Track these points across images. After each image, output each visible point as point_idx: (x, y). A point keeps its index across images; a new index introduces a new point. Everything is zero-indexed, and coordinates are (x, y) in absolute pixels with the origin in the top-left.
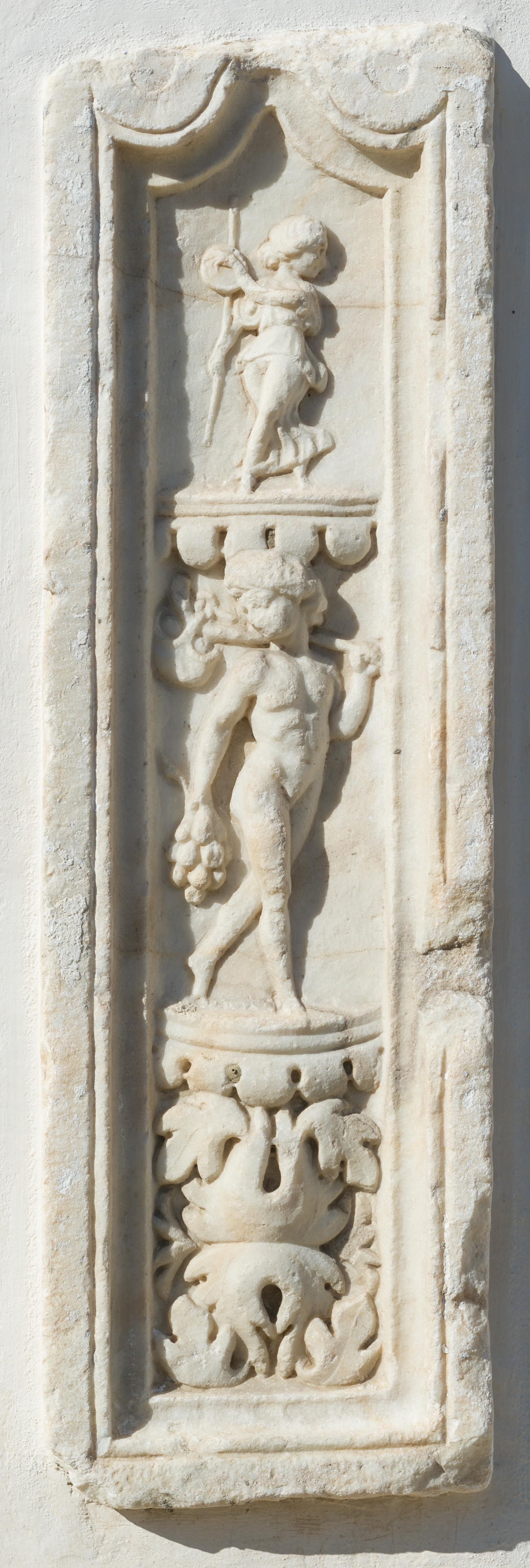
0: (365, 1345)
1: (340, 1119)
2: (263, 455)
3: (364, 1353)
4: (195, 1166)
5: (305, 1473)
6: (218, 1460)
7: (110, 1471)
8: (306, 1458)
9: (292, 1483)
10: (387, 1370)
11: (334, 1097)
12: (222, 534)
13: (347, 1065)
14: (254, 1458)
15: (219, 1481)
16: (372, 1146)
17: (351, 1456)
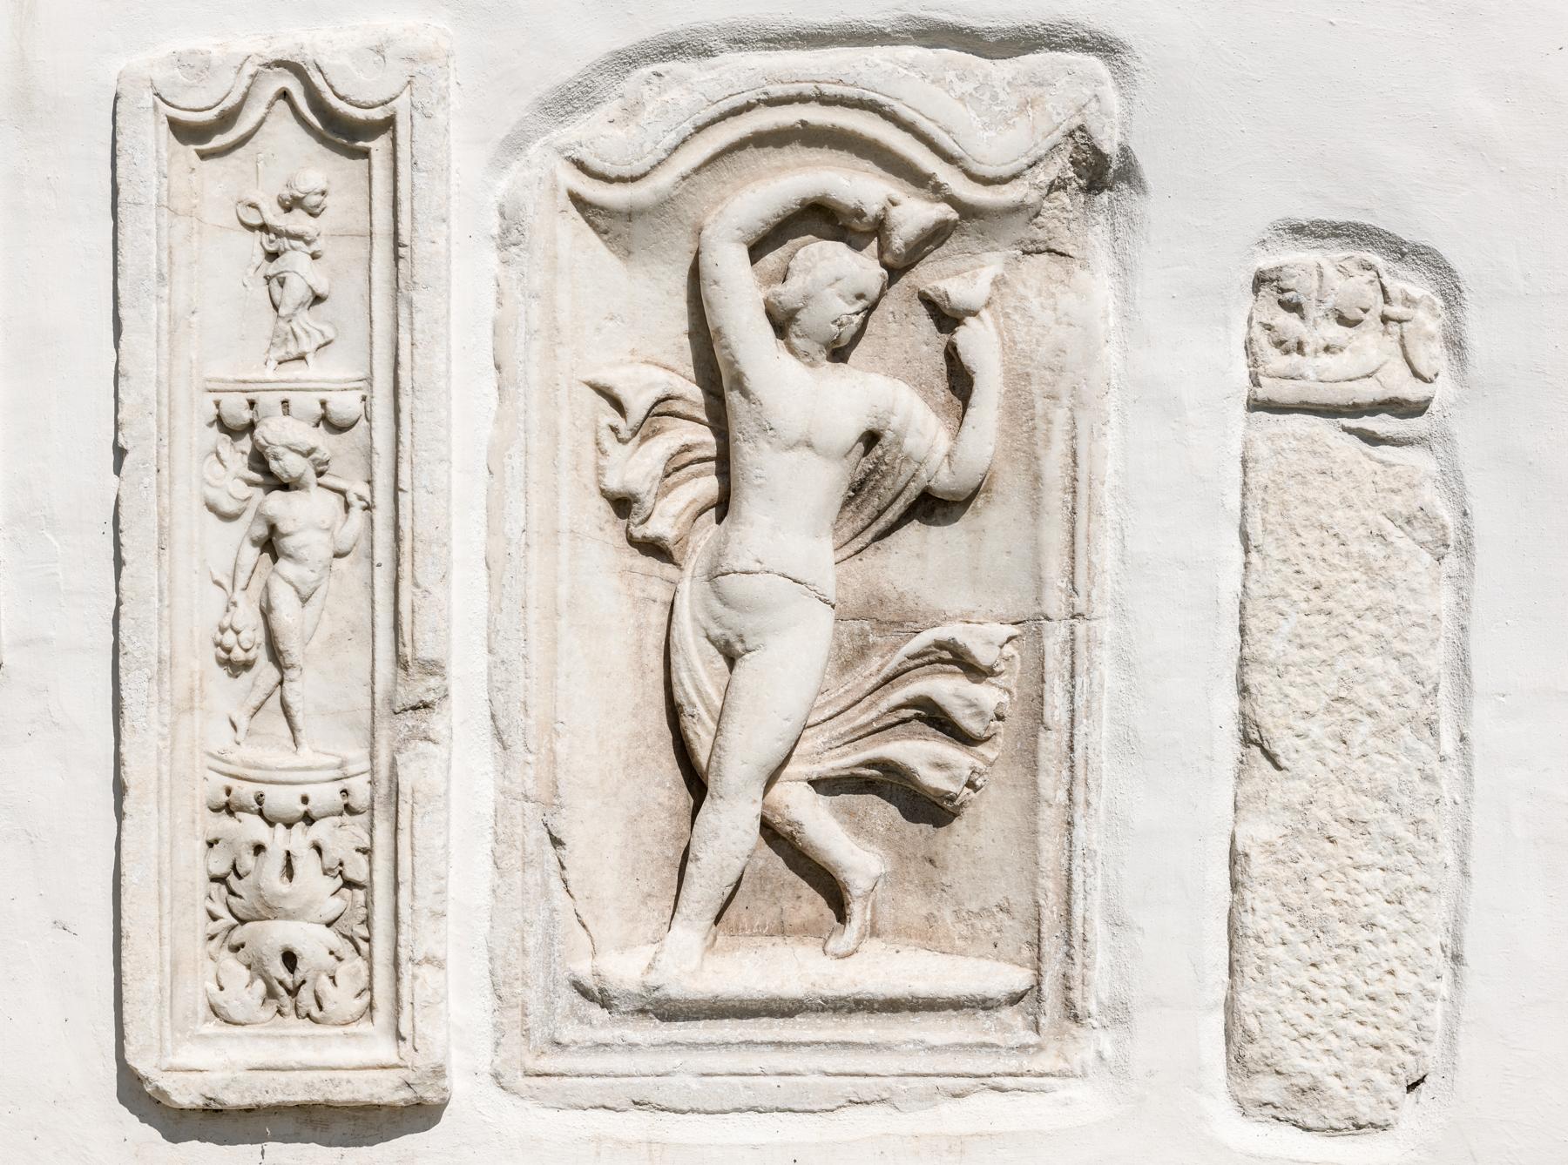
1: (338, 832)
5: (309, 1086)
12: (252, 404)
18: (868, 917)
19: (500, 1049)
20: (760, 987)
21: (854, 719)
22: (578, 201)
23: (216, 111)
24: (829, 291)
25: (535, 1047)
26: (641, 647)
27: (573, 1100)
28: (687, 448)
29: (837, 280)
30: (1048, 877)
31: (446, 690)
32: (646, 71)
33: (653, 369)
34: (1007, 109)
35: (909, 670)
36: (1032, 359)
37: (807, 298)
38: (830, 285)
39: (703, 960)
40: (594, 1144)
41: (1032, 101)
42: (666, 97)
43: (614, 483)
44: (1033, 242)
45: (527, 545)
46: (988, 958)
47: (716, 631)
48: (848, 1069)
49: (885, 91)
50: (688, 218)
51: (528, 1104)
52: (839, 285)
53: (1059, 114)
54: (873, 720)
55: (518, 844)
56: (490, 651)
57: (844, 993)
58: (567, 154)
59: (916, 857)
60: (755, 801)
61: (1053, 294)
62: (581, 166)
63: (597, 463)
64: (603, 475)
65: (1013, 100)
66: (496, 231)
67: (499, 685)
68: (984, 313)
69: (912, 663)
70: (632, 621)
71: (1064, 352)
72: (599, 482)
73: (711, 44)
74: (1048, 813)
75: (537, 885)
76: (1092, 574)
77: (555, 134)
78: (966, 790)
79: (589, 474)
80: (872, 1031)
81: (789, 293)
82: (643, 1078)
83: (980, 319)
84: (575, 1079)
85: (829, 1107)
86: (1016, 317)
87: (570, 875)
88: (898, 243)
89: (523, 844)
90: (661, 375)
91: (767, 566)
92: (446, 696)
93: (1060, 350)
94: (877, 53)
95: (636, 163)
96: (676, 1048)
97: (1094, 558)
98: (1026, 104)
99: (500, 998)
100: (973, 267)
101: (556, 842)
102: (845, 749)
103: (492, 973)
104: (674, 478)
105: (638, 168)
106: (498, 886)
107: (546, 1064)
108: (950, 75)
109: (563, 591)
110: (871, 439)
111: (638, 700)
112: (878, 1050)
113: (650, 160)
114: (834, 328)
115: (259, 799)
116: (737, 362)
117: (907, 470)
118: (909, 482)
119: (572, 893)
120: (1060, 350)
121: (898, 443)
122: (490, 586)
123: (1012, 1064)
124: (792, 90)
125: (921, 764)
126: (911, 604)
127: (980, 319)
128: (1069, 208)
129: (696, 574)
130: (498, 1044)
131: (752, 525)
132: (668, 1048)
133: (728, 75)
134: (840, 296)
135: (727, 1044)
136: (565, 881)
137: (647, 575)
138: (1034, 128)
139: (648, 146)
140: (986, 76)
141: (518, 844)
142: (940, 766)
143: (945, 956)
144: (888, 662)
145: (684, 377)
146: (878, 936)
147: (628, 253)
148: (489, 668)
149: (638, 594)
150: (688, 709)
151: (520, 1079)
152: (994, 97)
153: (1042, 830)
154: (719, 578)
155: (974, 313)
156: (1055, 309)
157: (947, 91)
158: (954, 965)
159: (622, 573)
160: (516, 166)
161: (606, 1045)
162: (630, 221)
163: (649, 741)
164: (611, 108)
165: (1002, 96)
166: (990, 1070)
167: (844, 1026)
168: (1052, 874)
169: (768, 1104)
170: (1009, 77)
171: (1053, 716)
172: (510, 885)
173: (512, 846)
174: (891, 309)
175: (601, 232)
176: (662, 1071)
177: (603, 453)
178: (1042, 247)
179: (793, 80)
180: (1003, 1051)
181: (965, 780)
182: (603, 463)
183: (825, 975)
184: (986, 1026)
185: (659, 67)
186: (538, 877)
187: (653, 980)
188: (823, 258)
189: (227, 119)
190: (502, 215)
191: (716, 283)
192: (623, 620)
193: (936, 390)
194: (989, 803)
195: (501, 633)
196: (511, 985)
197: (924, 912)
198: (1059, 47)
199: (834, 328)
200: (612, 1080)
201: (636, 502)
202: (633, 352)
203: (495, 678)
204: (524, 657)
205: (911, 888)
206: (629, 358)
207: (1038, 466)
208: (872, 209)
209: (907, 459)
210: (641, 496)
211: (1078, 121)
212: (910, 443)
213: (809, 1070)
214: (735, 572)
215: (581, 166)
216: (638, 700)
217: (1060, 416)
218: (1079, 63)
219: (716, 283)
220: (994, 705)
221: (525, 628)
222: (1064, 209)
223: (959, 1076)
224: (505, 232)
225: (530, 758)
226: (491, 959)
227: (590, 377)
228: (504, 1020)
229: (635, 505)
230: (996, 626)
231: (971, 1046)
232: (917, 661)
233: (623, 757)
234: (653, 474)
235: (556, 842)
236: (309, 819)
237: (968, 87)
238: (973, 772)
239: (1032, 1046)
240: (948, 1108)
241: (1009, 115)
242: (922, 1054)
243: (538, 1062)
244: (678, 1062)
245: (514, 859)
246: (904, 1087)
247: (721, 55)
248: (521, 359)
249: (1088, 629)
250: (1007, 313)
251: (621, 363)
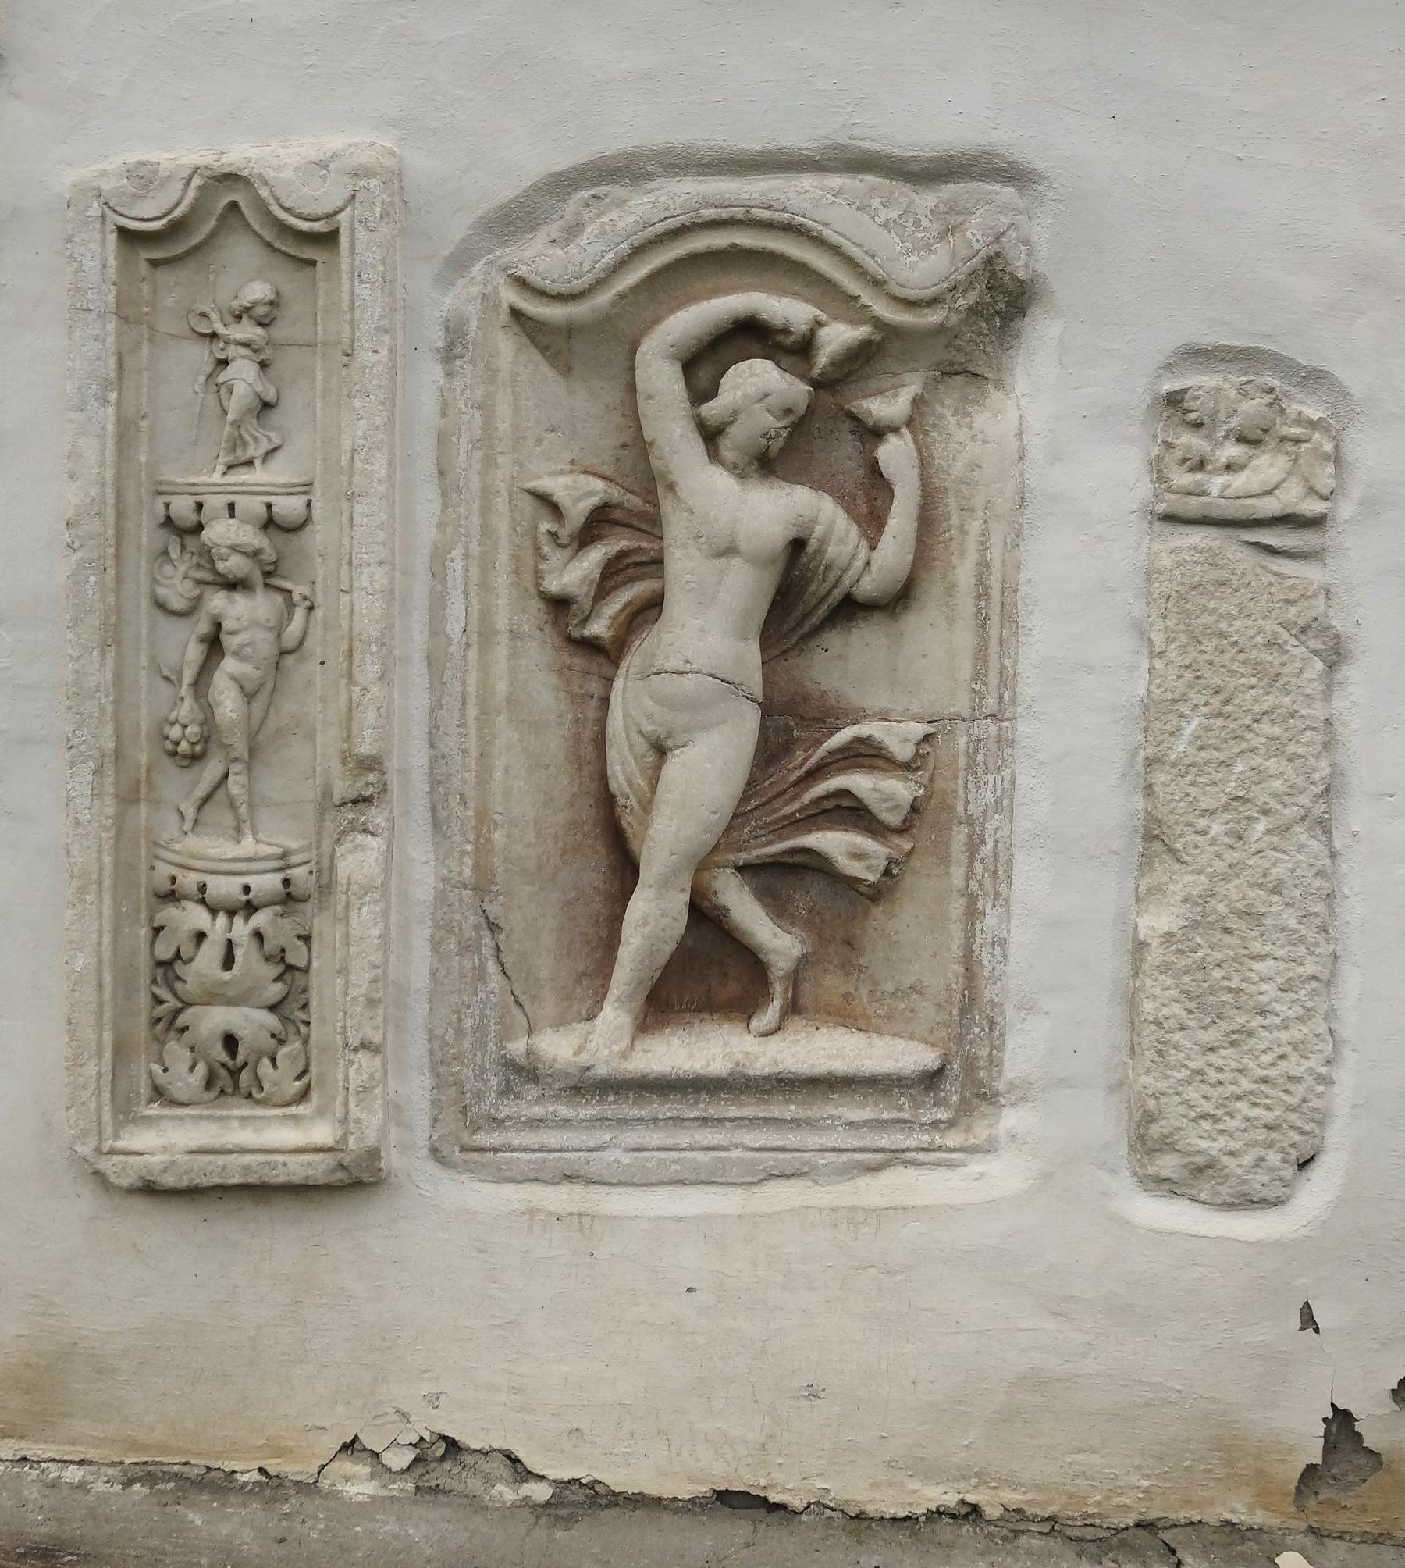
0: (299, 1077)
2: (233, 449)
3: (297, 1083)
4: (178, 951)
5: (246, 1169)
6: (187, 1157)
7: (110, 1163)
8: (247, 1159)
9: (237, 1176)
10: (315, 1095)
11: (275, 904)
13: (286, 882)
14: (211, 1158)
15: (186, 1173)
16: (306, 939)
17: (280, 1158)
18: (790, 995)
19: (437, 1125)
20: (686, 1067)
21: (779, 809)
22: (516, 313)
23: (163, 222)
24: (757, 406)
25: (472, 1122)
26: (578, 740)
27: (508, 1174)
29: (766, 395)
31: (385, 784)
32: (586, 194)
33: (591, 478)
34: (928, 235)
35: (831, 763)
38: (760, 400)
39: (633, 1040)
40: (527, 1217)
41: (954, 228)
42: (604, 219)
43: (554, 585)
44: (951, 364)
45: (467, 644)
46: (902, 1037)
47: (648, 728)
48: (770, 1144)
49: (814, 217)
51: (464, 1178)
52: (768, 400)
53: (978, 241)
54: (796, 811)
55: (456, 930)
56: (432, 745)
57: (767, 1071)
58: (510, 272)
59: (834, 939)
60: (683, 890)
61: (970, 413)
62: (522, 283)
63: (536, 567)
64: (543, 578)
65: (935, 228)
66: (440, 344)
67: (439, 778)
68: (904, 430)
69: (833, 759)
70: (570, 716)
72: (538, 585)
73: (649, 169)
75: (474, 968)
76: (1004, 677)
77: (498, 253)
79: (528, 577)
80: (792, 1107)
82: (575, 1154)
84: (509, 1154)
85: (750, 1179)
86: (935, 434)
87: (508, 959)
89: (461, 929)
90: (599, 485)
92: (385, 790)
93: (977, 466)
94: (807, 182)
95: (575, 281)
96: (607, 1123)
97: (1007, 663)
98: (947, 232)
99: (438, 1076)
100: (894, 387)
101: (494, 927)
102: (770, 837)
103: (431, 1053)
104: (609, 584)
105: (577, 285)
106: (437, 970)
107: (482, 1138)
108: (876, 203)
109: (502, 688)
110: (798, 545)
111: (575, 790)
112: (799, 1126)
113: (589, 279)
114: (764, 442)
115: (203, 888)
117: (832, 577)
119: (509, 974)
121: (820, 551)
122: (431, 683)
123: (925, 1139)
124: (725, 214)
126: (834, 702)
128: (986, 332)
129: (630, 672)
130: (435, 1120)
132: (599, 1123)
133: (662, 199)
134: (768, 411)
135: (655, 1120)
136: (502, 965)
137: (585, 673)
138: (953, 255)
139: (586, 267)
140: (909, 205)
141: (456, 930)
142: (858, 856)
143: (861, 1034)
144: (810, 756)
145: (621, 487)
146: (799, 1013)
147: (566, 371)
148: (431, 762)
149: (576, 690)
150: (621, 801)
151: (457, 1154)
152: (917, 224)
155: (896, 430)
156: (971, 427)
157: (873, 218)
159: (560, 673)
160: (460, 283)
161: (541, 1121)
163: (586, 828)
164: (554, 229)
165: (925, 223)
166: (903, 1146)
167: (766, 1102)
169: (693, 1178)
170: (931, 205)
171: (966, 810)
172: (448, 968)
173: (451, 932)
175: (543, 349)
176: (591, 1144)
177: (544, 558)
178: (960, 369)
179: (726, 204)
180: (916, 1127)
181: (882, 869)
182: (543, 567)
183: (748, 1053)
184: (901, 1102)
185: (600, 190)
186: (476, 960)
187: (584, 1059)
188: (752, 375)
189: (177, 228)
190: (447, 328)
192: (561, 716)
193: (857, 502)
195: (441, 729)
196: (449, 1065)
197: (842, 990)
198: (981, 177)
199: (764, 442)
200: (545, 1155)
202: (573, 462)
203: (435, 771)
204: (464, 751)
205: (831, 967)
206: (568, 467)
211: (995, 248)
212: (832, 551)
213: (732, 1145)
215: (522, 283)
216: (575, 790)
217: (975, 526)
218: (997, 193)
220: (910, 799)
221: (464, 725)
222: (981, 334)
223: (874, 1151)
224: (450, 346)
225: (469, 848)
226: (430, 1040)
227: (530, 485)
228: (443, 1098)
230: (913, 724)
231: (886, 1121)
232: (839, 756)
233: (560, 844)
234: (591, 578)
235: (494, 927)
236: (250, 908)
237: (893, 214)
238: (890, 862)
239: (943, 1122)
240: (863, 1182)
241: (931, 241)
242: (840, 1128)
243: (474, 1137)
244: (607, 1137)
245: (452, 944)
246: (823, 1162)
247: (659, 180)
248: (464, 466)
249: (1000, 729)
251: (561, 472)
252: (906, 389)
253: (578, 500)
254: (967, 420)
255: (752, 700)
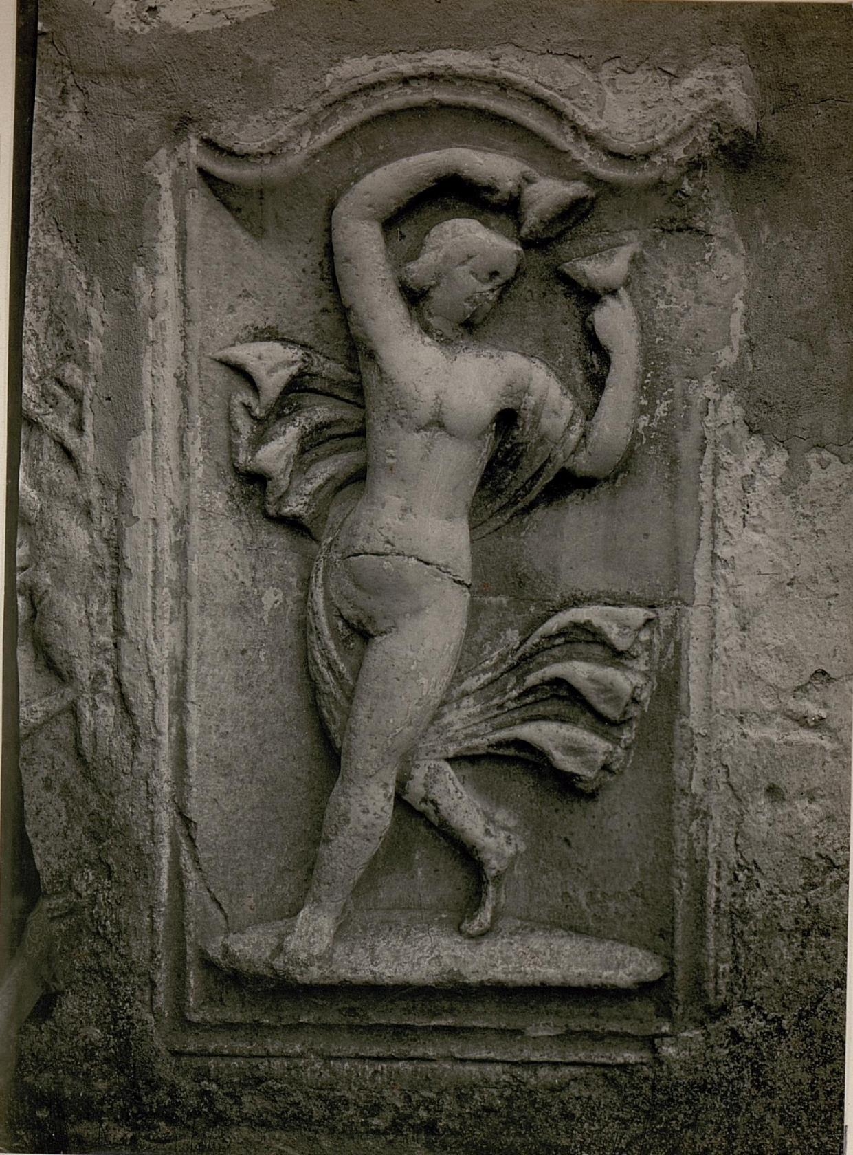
28: (320, 427)
29: (470, 257)
30: (683, 866)
36: (671, 339)
37: (438, 276)
38: (463, 263)
50: (322, 196)
61: (693, 273)
68: (622, 291)
71: (704, 332)
74: (684, 802)
78: (602, 774)
81: (420, 270)
83: (620, 300)
88: (532, 218)
91: (398, 547)
100: (611, 246)
110: (506, 419)
116: (370, 340)
118: (545, 462)
120: (700, 330)
125: (556, 748)
127: (620, 300)
131: (383, 505)
134: (472, 273)
142: (575, 750)
147: (257, 231)
153: (677, 819)
154: (351, 558)
155: (613, 293)
158: (587, 948)
162: (261, 198)
168: (686, 864)
174: (529, 287)
175: (235, 211)
188: (455, 235)
191: (348, 260)
194: (624, 785)
201: (270, 479)
207: (676, 448)
208: (507, 185)
209: (542, 440)
210: (274, 475)
212: (546, 423)
214: (366, 554)
219: (348, 260)
227: (219, 355)
229: (269, 483)
250: (645, 291)
252: (624, 248)
253: (272, 371)
254: (691, 280)
255: (460, 582)
